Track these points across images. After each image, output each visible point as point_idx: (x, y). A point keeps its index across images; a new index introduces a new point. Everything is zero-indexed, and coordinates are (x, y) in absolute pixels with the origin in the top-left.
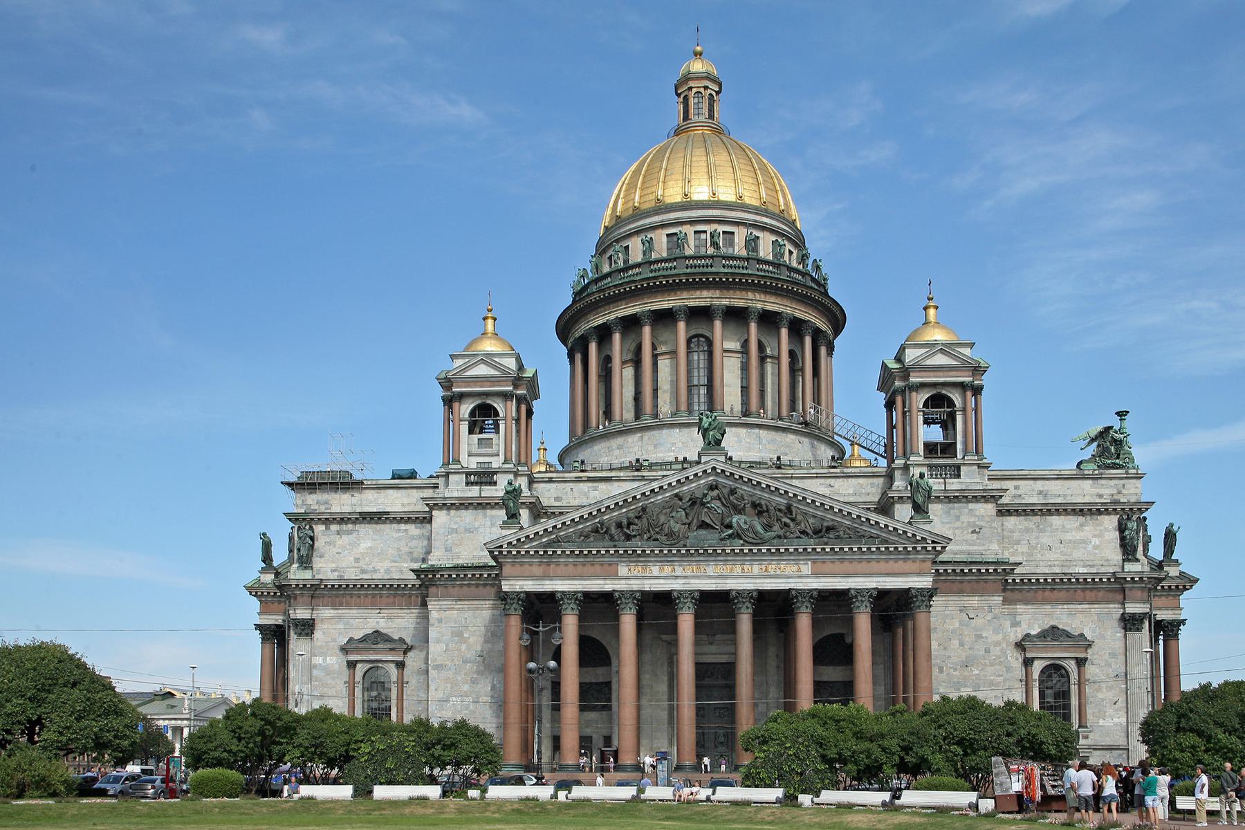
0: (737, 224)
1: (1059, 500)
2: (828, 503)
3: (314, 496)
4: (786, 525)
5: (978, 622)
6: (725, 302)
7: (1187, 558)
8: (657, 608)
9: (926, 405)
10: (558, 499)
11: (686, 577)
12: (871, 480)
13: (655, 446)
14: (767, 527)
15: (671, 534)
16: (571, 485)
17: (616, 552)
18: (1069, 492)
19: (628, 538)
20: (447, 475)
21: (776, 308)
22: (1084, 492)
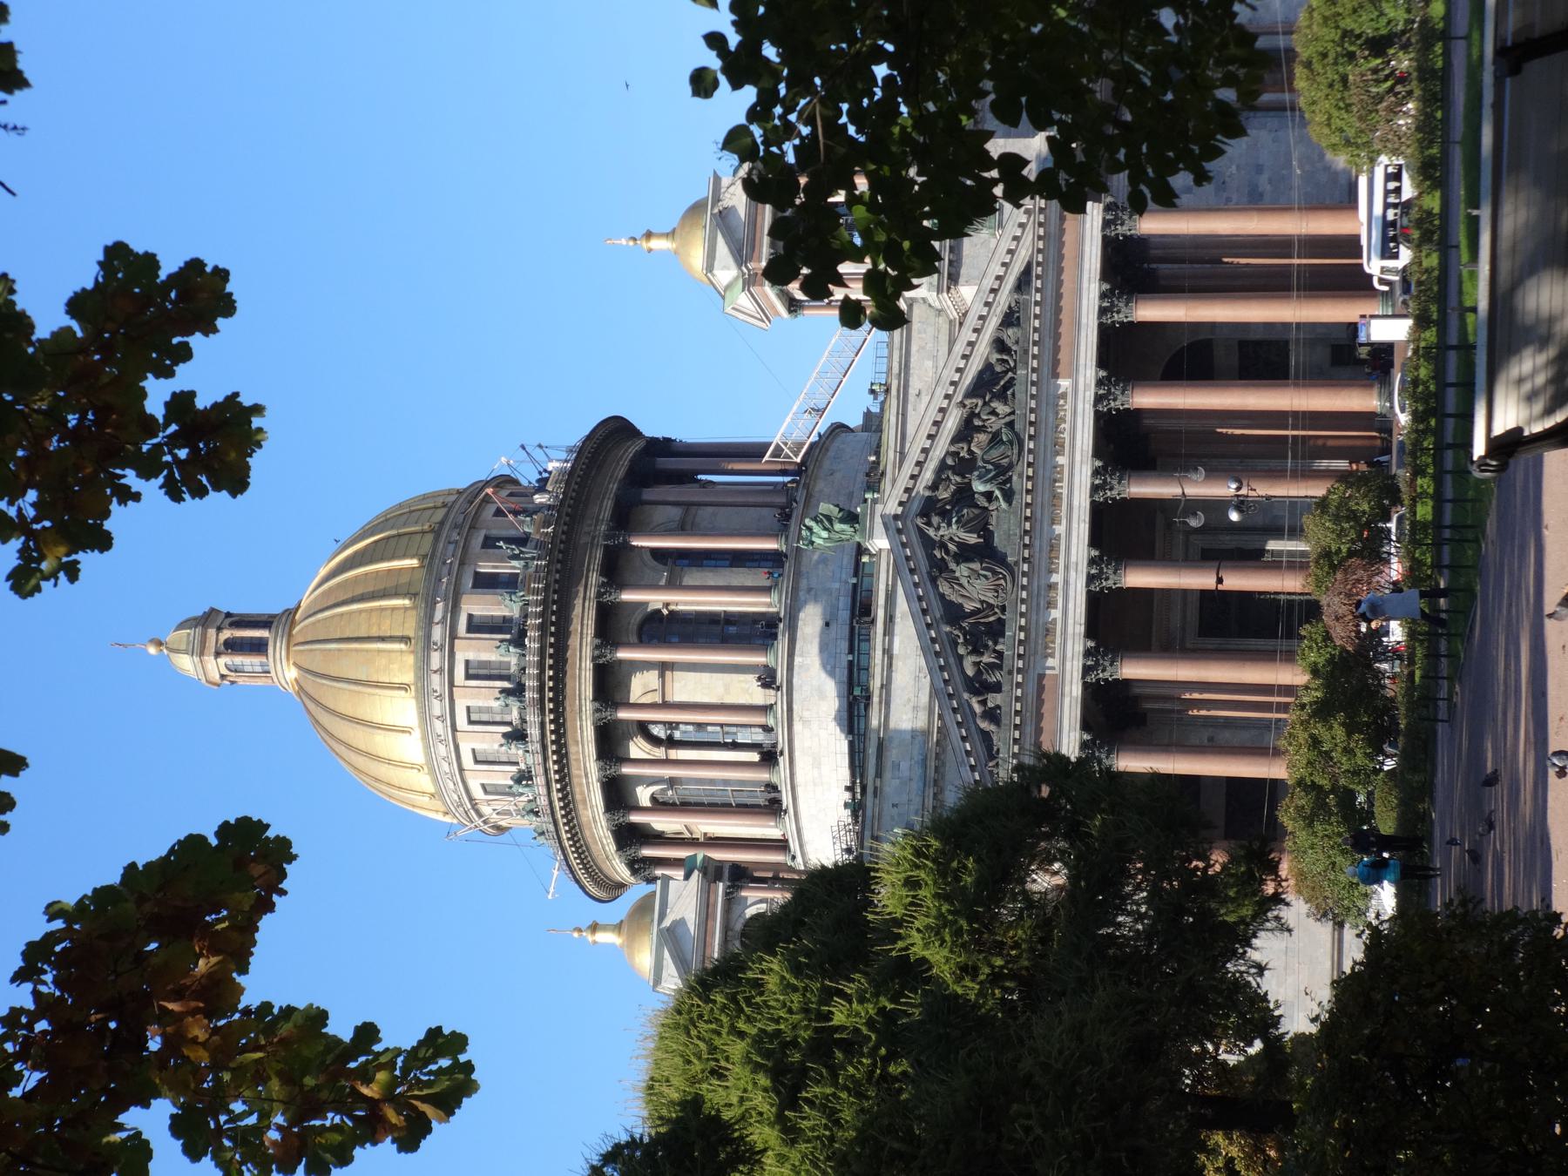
0: (462, 563)
2: (960, 348)
6: (594, 578)
11: (1067, 568)
16: (887, 807)
17: (1019, 671)
21: (608, 504)
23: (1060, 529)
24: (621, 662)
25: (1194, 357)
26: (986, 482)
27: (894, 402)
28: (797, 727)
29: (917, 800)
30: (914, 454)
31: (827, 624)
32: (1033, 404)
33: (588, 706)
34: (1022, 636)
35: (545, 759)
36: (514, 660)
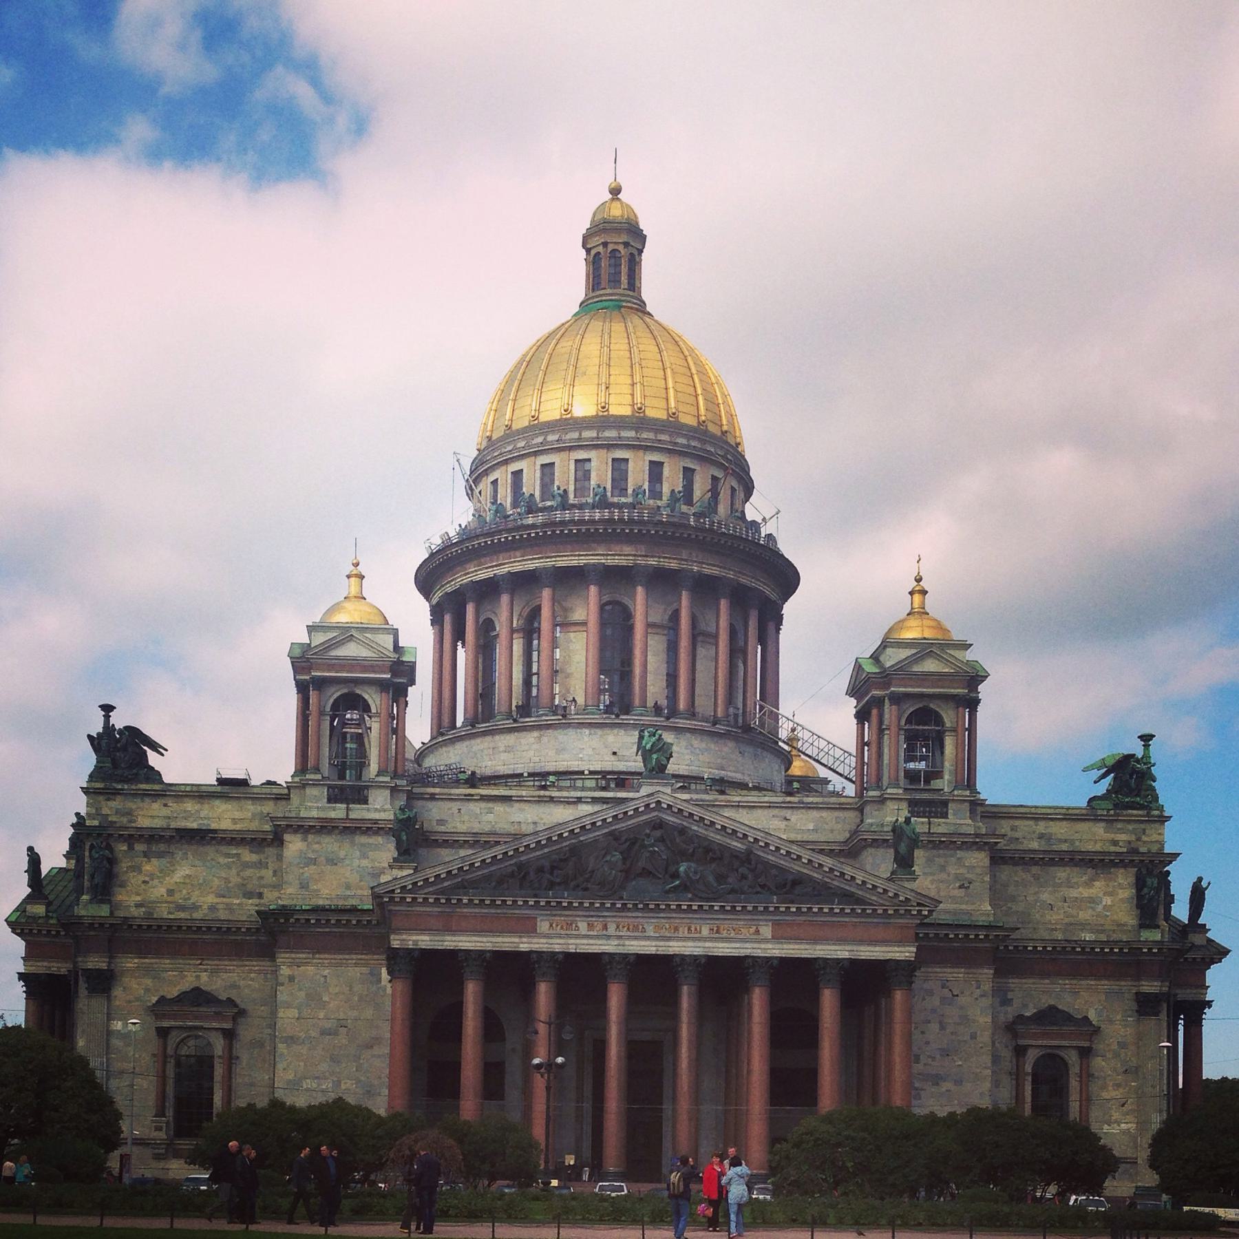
1: (1064, 847)
3: (113, 804)
4: (744, 877)
5: (963, 1000)
6: (653, 562)
7: (1218, 924)
8: (581, 976)
9: (908, 721)
10: (441, 822)
11: (620, 937)
12: (837, 813)
13: (558, 752)
14: (721, 878)
15: (602, 884)
18: (1077, 836)
19: (552, 885)
20: (303, 786)
22: (1095, 837)
23: (650, 932)
24: (588, 588)
25: (793, 1031)
26: (686, 871)
27: (780, 799)
28: (536, 734)
29: (462, 828)
30: (708, 817)
31: (615, 753)
32: (750, 908)
33: (549, 563)
34: (565, 904)
35: (509, 531)
36: (590, 500)
